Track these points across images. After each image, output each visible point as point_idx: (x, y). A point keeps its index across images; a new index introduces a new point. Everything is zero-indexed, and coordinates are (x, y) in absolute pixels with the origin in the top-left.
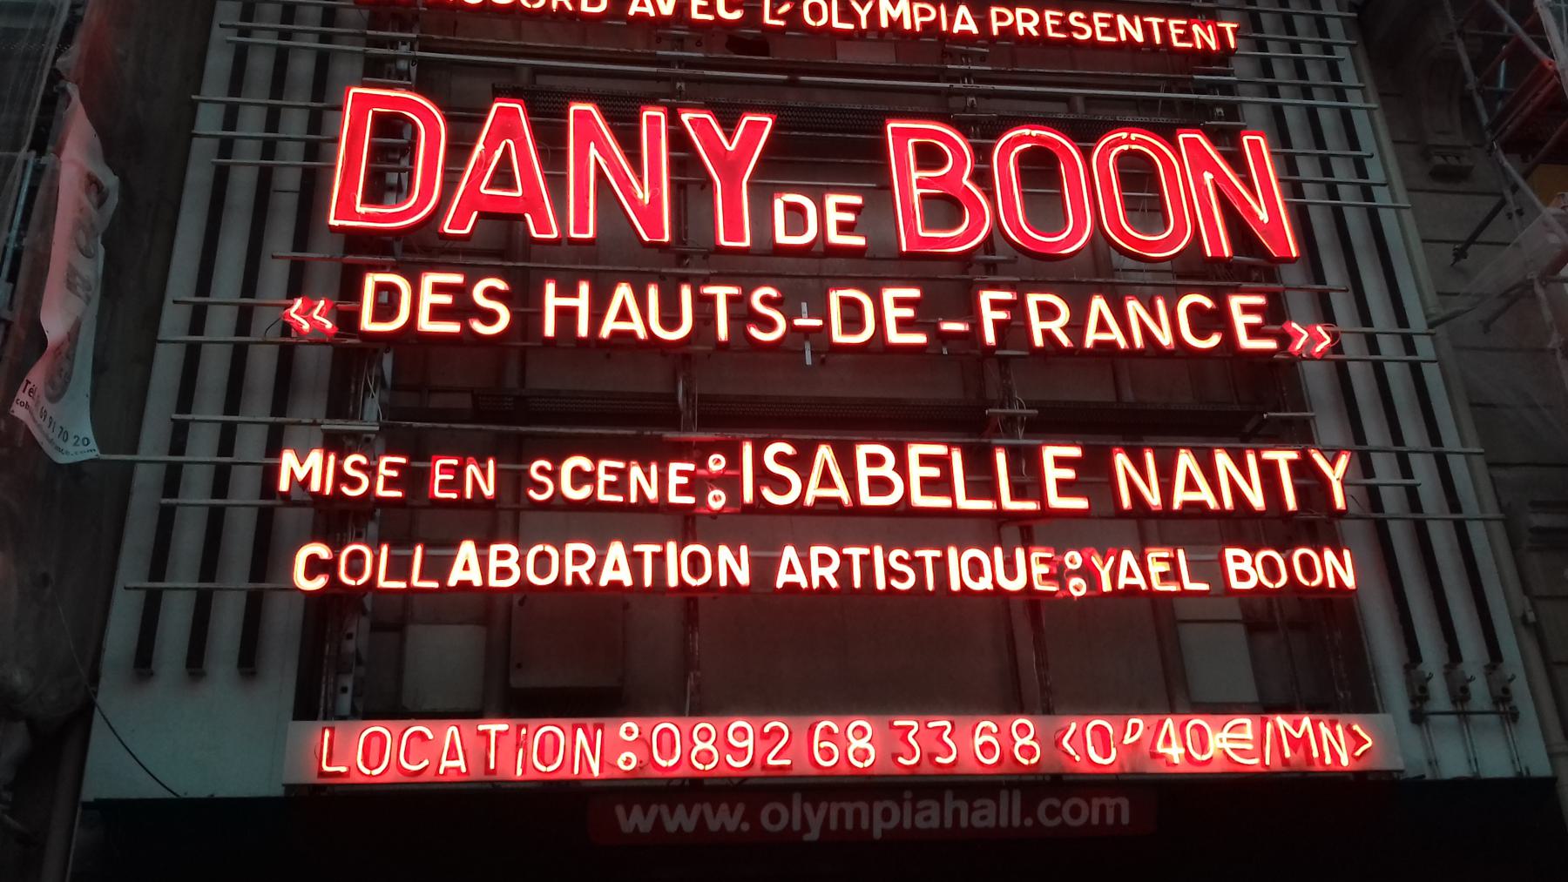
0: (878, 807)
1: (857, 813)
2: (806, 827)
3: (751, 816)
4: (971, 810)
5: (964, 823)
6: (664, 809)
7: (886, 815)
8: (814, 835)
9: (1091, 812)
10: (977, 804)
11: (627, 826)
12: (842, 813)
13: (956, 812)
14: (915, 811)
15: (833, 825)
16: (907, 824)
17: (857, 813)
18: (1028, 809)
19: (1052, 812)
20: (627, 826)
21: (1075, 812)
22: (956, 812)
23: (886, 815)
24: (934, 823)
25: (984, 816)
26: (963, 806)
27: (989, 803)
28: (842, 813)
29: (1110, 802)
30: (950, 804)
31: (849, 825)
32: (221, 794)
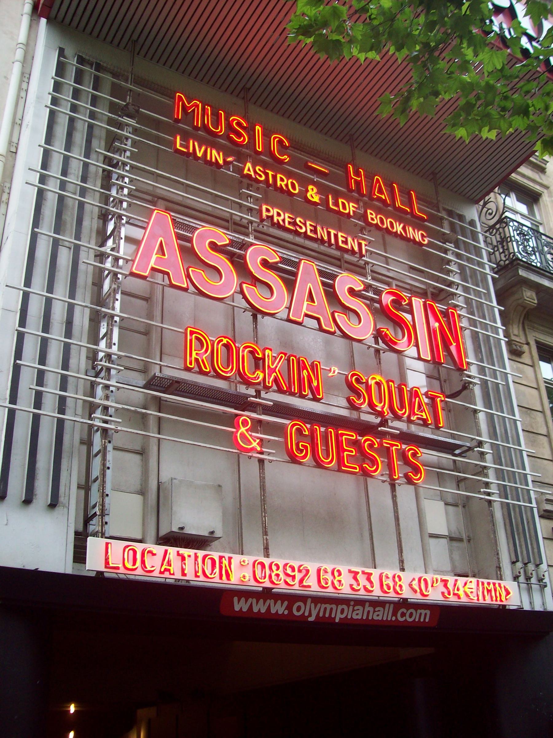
2: (310, 615)
4: (374, 611)
6: (254, 601)
7: (342, 611)
10: (377, 609)
11: (237, 608)
13: (369, 612)
14: (353, 610)
15: (321, 615)
16: (349, 617)
20: (237, 608)
22: (369, 612)
23: (342, 611)
25: (379, 615)
26: (371, 609)
27: (381, 609)
31: (327, 615)
32: (41, 569)
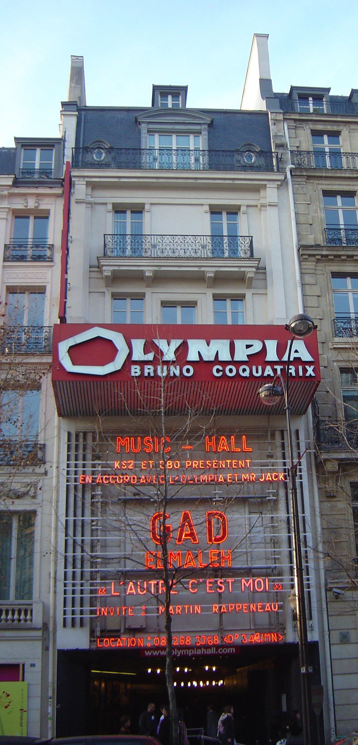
0: (190, 651)
1: (186, 652)
2: (177, 654)
5: (205, 653)
7: (192, 652)
8: (179, 655)
9: (228, 651)
12: (184, 652)
17: (186, 652)
18: (217, 650)
21: (225, 651)
23: (192, 652)
24: (200, 653)
26: (205, 650)
28: (184, 652)
29: (231, 649)
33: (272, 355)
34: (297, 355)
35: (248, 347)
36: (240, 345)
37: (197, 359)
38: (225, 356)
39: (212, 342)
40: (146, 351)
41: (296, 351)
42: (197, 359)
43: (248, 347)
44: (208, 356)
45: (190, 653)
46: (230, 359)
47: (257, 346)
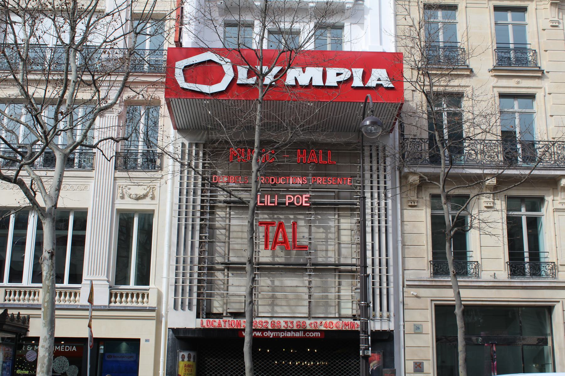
3: (262, 334)
8: (271, 337)
9: (314, 334)
18: (304, 334)
19: (308, 334)
21: (312, 334)
30: (292, 333)
33: (357, 82)
34: (379, 82)
35: (338, 74)
36: (332, 72)
37: (294, 83)
38: (318, 81)
39: (308, 69)
40: (250, 75)
41: (379, 80)
42: (294, 83)
43: (338, 74)
44: (304, 80)
45: (281, 335)
46: (322, 84)
47: (346, 74)
